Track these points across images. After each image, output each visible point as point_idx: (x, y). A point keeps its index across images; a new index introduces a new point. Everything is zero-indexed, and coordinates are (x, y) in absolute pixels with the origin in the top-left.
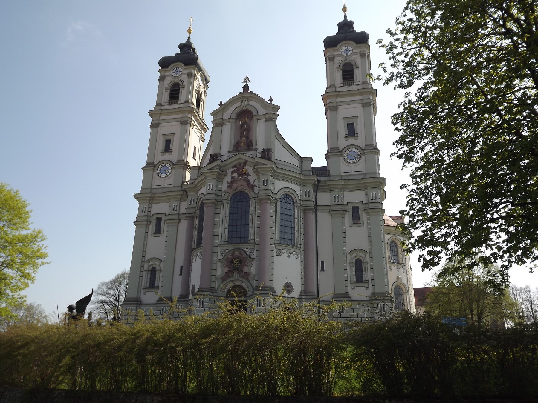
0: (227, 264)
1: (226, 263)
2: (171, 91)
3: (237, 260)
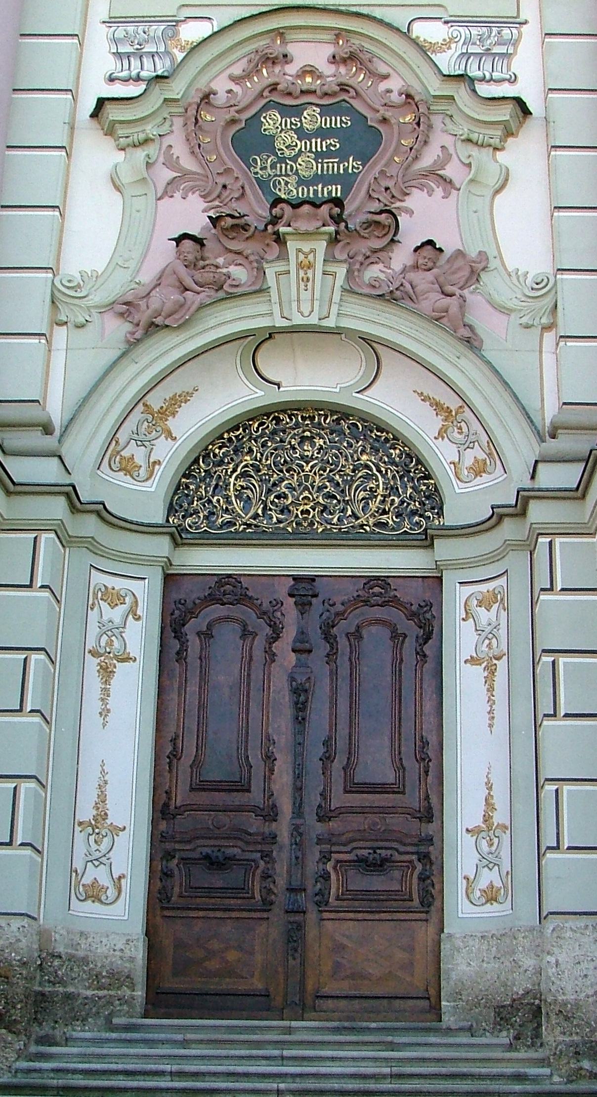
0: (188, 164)
1: (180, 150)
3: (311, 118)
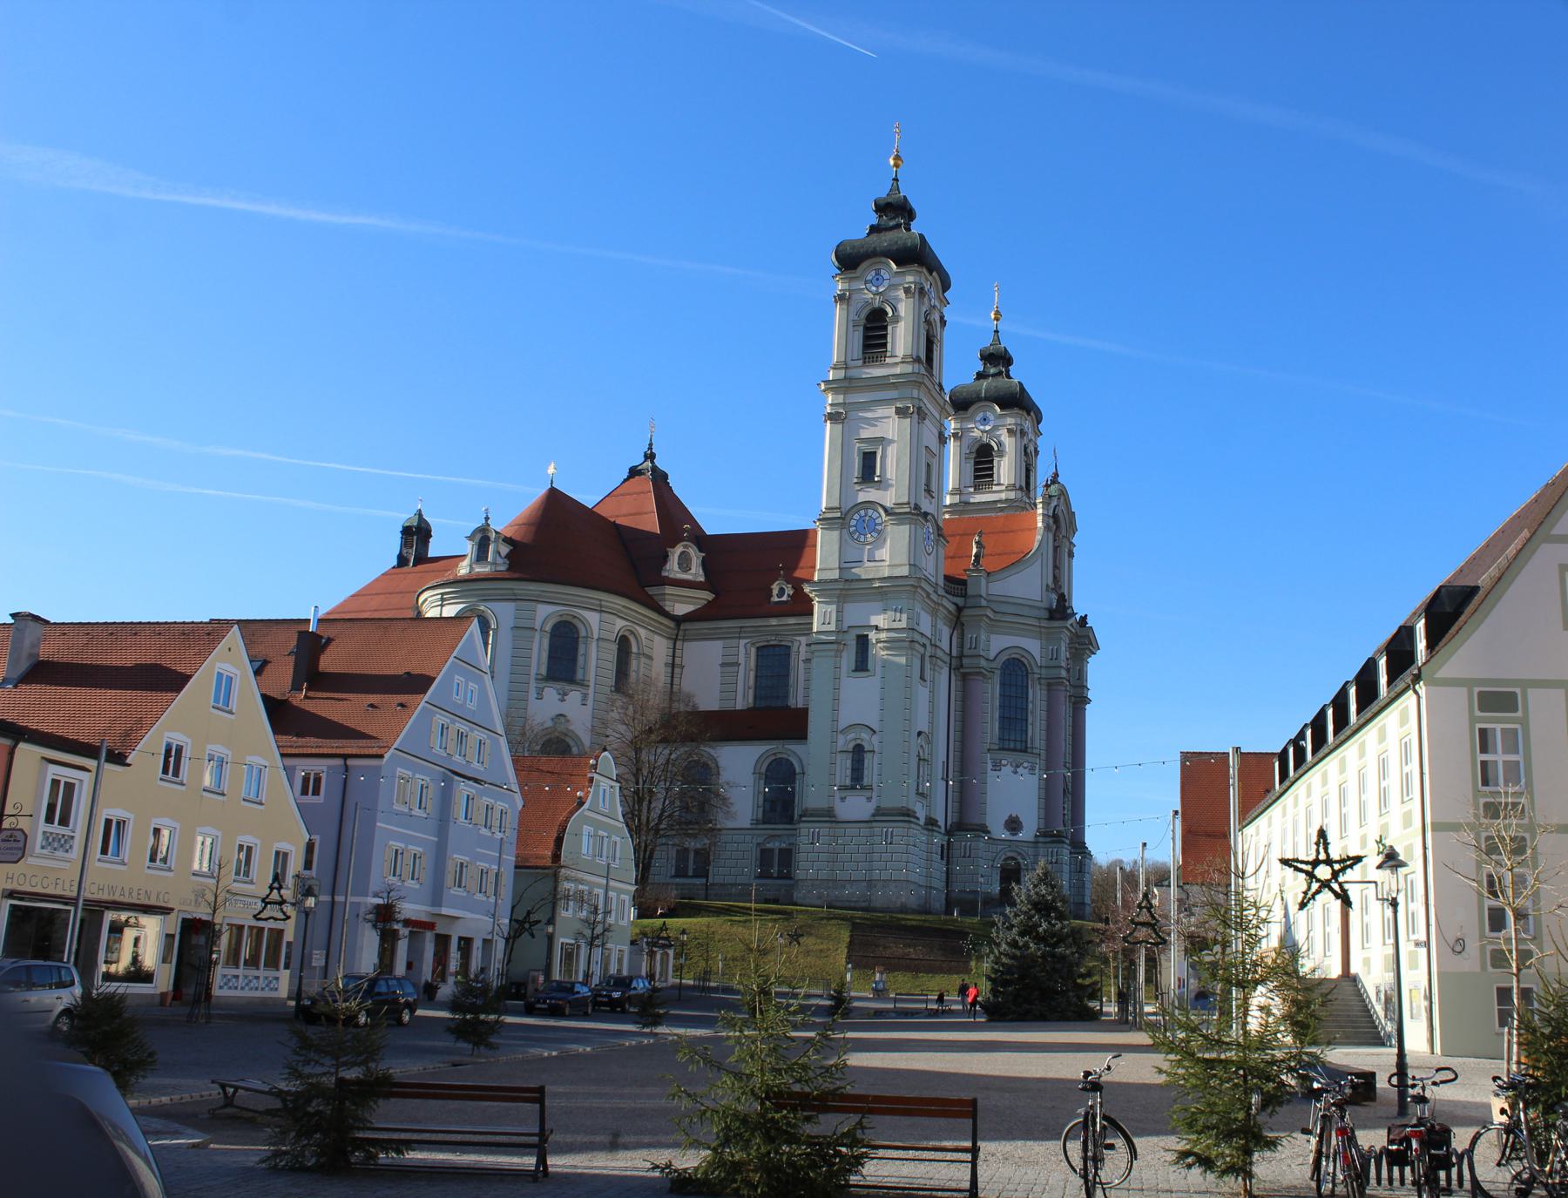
2: (866, 329)
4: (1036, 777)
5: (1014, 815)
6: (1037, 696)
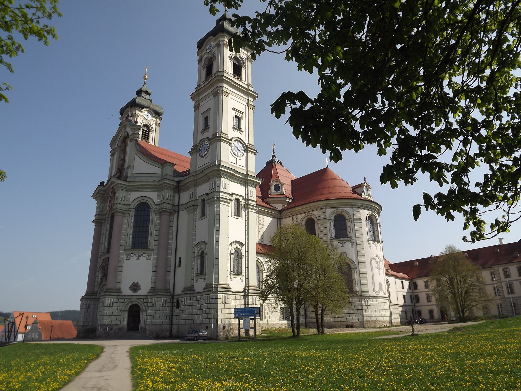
4: (152, 260)
5: (136, 282)
6: (154, 220)
